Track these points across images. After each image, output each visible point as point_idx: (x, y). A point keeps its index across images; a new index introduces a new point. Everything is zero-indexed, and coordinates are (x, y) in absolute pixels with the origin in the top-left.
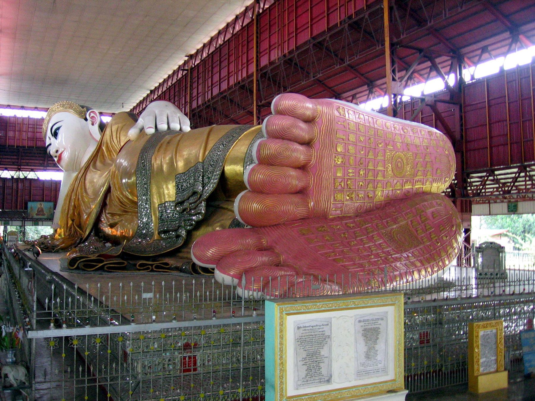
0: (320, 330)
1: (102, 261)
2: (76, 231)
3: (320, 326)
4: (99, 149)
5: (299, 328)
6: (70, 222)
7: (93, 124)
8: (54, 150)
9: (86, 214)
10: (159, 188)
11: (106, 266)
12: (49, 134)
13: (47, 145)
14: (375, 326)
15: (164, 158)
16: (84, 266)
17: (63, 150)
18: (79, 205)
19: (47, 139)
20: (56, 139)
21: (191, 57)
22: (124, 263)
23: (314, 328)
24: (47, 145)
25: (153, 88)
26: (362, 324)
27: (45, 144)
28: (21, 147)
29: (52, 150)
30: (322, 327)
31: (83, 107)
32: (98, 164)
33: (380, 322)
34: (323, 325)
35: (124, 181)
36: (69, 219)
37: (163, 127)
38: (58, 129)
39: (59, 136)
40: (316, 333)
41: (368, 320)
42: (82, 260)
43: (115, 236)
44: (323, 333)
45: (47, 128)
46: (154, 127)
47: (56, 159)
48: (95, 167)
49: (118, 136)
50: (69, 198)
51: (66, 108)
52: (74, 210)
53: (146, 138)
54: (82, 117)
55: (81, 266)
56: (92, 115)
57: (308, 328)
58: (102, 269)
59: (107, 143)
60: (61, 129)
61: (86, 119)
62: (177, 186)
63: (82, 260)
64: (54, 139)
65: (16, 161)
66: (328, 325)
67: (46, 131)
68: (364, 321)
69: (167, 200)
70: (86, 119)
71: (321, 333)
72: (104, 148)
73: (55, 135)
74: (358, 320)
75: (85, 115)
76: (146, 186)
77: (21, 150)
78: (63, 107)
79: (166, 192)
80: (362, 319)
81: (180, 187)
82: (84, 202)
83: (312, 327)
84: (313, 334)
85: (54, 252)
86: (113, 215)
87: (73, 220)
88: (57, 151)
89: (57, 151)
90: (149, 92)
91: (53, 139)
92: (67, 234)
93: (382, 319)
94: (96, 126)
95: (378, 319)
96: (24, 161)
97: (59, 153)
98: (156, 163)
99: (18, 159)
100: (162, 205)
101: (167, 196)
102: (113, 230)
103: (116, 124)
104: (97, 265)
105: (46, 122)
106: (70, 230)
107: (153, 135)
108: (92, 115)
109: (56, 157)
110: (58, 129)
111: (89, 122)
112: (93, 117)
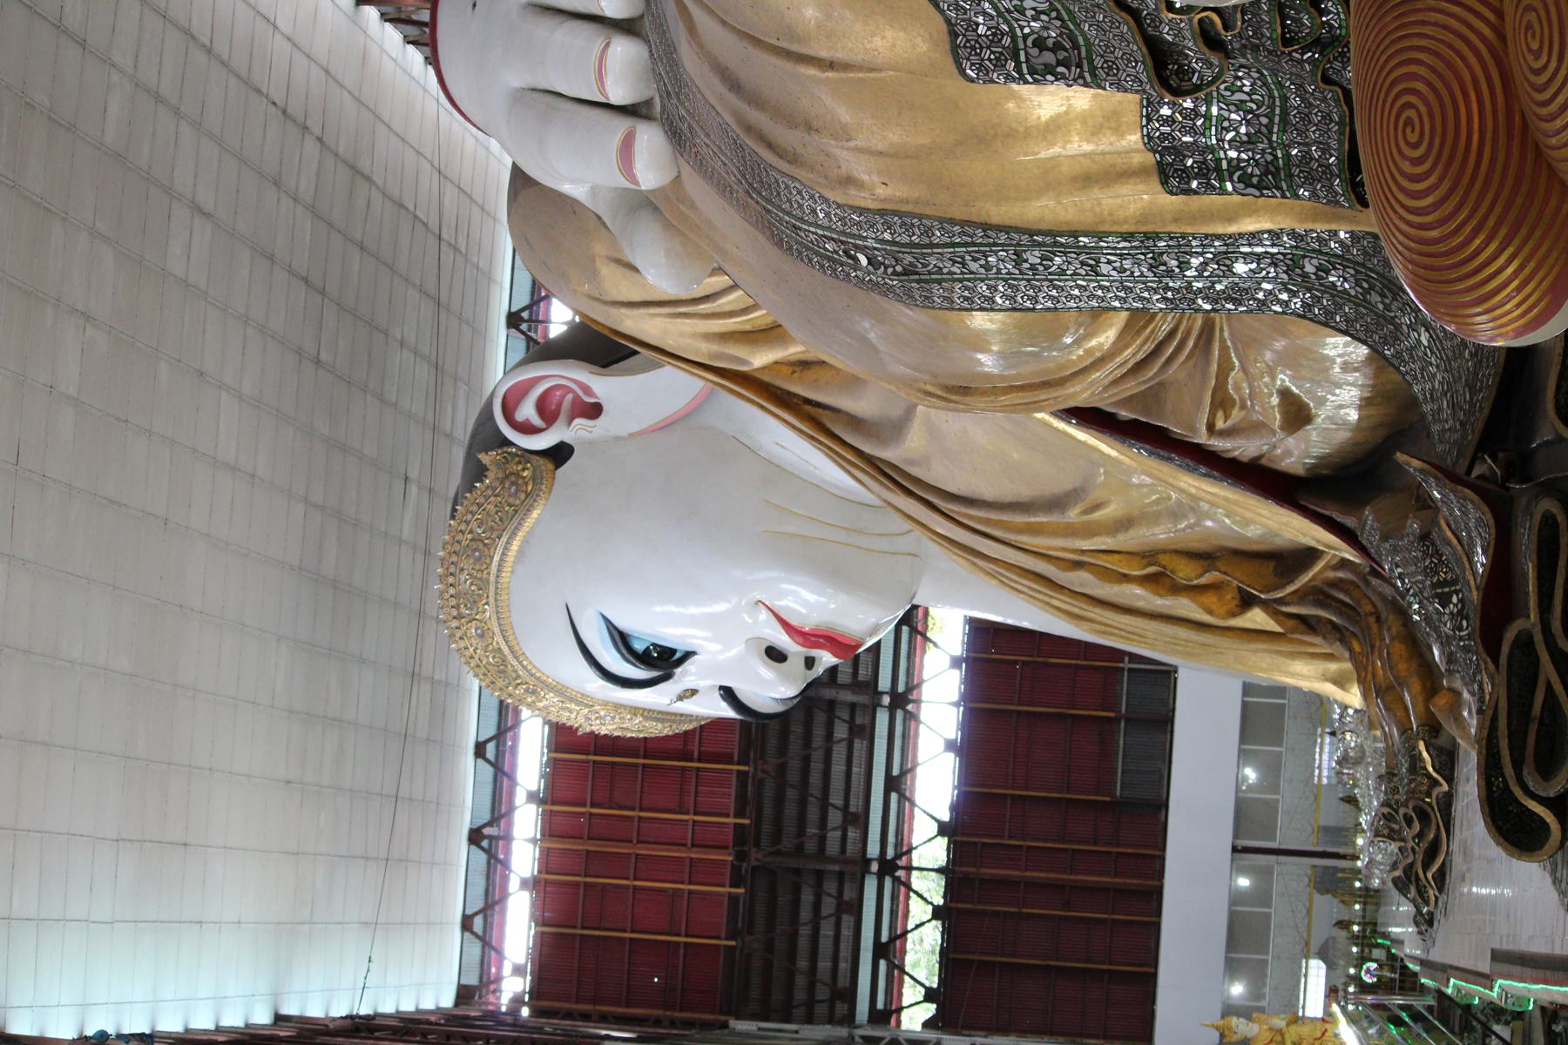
1: (1525, 644)
2: (1316, 594)
4: (768, 391)
6: (1257, 618)
7: (594, 411)
10: (1049, 179)
12: (658, 697)
13: (728, 712)
15: (843, 134)
17: (764, 615)
18: (1149, 555)
19: (687, 707)
20: (688, 655)
24: (728, 712)
27: (718, 724)
28: (741, 856)
29: (771, 690)
31: (475, 472)
32: (861, 405)
38: (621, 640)
39: (672, 635)
42: (1509, 770)
43: (1365, 404)
45: (618, 707)
46: (622, 124)
47: (827, 659)
51: (483, 584)
52: (1177, 589)
53: (699, 191)
56: (527, 411)
59: (725, 337)
62: (1040, 74)
63: (1509, 770)
64: (689, 666)
65: (831, 886)
67: (635, 710)
69: (1134, 139)
70: (560, 454)
72: (759, 359)
73: (663, 661)
76: (1033, 257)
77: (756, 856)
81: (1049, 58)
85: (1450, 780)
88: (775, 655)
89: (775, 655)
91: (686, 676)
92: (1337, 648)
96: (834, 836)
97: (783, 641)
98: (879, 188)
101: (1106, 143)
102: (1322, 415)
103: (594, 275)
104: (1549, 686)
106: (1308, 624)
108: (527, 411)
109: (810, 662)
110: (621, 640)
112: (542, 406)
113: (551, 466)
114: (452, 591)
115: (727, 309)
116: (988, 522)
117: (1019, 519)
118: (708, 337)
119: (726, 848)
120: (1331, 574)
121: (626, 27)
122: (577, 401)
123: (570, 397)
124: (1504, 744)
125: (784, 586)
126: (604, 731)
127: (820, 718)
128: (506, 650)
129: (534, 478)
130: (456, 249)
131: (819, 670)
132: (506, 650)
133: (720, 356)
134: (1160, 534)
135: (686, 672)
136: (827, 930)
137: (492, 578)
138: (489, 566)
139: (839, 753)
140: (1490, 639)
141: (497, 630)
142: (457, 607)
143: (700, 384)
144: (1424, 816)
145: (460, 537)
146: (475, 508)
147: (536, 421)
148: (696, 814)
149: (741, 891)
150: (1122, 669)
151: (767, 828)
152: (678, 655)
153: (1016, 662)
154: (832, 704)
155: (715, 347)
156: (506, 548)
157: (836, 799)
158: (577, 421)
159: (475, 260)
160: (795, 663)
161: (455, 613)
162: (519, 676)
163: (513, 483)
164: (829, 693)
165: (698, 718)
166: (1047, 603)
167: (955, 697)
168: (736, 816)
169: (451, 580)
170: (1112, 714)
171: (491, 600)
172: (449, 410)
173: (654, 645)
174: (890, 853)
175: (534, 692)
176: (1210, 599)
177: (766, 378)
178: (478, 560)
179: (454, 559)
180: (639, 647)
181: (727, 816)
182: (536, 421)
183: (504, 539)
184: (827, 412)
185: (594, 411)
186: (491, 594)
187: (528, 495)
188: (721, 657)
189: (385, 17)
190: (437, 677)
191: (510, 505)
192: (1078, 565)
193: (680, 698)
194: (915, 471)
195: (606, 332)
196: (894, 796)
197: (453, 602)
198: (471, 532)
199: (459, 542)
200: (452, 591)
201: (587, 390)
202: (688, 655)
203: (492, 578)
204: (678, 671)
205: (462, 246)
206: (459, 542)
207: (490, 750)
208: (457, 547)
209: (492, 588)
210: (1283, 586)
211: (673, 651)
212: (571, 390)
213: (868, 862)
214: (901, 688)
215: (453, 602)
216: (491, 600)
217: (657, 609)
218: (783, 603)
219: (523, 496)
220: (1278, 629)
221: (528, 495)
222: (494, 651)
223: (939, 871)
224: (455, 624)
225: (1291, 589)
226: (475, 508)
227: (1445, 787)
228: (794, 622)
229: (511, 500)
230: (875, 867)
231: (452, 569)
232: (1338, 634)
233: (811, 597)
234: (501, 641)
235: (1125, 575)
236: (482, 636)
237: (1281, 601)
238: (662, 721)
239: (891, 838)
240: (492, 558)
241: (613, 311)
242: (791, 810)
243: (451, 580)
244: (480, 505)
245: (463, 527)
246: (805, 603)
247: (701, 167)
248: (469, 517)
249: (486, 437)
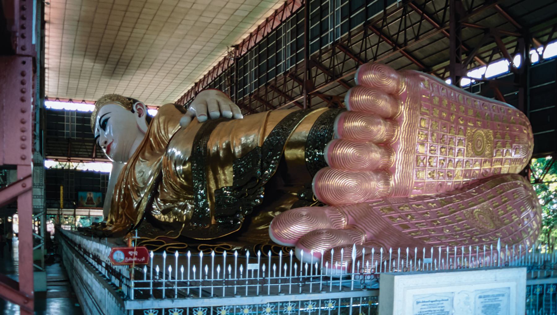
0: (440, 305)
3: (439, 301)
4: (147, 140)
5: (418, 303)
7: (140, 116)
8: (103, 141)
9: (137, 202)
14: (495, 303)
17: (111, 141)
21: (237, 47)
23: (434, 303)
25: (197, 81)
26: (482, 300)
29: (101, 141)
30: (441, 302)
31: (130, 99)
32: (147, 154)
33: (501, 298)
34: (443, 300)
35: (178, 168)
36: (120, 208)
37: (215, 114)
39: (108, 128)
40: (435, 309)
41: (488, 296)
44: (442, 309)
46: (206, 114)
47: (105, 151)
48: (144, 158)
49: (166, 127)
50: (402, 69)
51: (113, 100)
54: (129, 109)
56: (139, 107)
57: (428, 303)
64: (103, 131)
66: (447, 300)
67: (95, 122)
68: (485, 297)
71: (440, 309)
72: (151, 139)
73: (103, 126)
74: (478, 296)
75: (132, 106)
78: (110, 99)
79: (223, 177)
80: (482, 295)
83: (432, 302)
84: (432, 309)
88: (106, 142)
90: (193, 85)
91: (101, 131)
93: (503, 295)
94: (143, 118)
95: (499, 295)
97: (108, 144)
100: (219, 191)
102: (166, 217)
107: (205, 123)
108: (139, 107)
109: (105, 148)
110: (106, 120)
111: (136, 114)
121: (221, 115)
136: (60, 152)
139: (86, 153)
157: (80, 153)
185: (140, 116)
189: (192, 87)
247: (204, 125)
249: (135, 101)
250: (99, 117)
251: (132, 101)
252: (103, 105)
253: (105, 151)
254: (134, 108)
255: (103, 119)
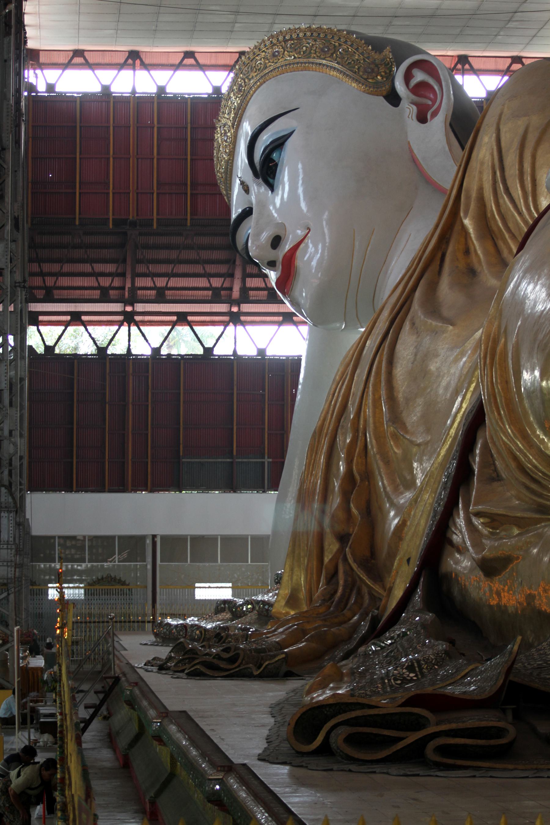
1: (417, 724)
2: (353, 584)
6: (332, 547)
7: (422, 119)
8: (265, 236)
9: (399, 510)
11: (432, 745)
16: (350, 740)
17: (300, 233)
18: (368, 476)
20: (272, 187)
22: (499, 732)
24: (234, 216)
27: (228, 209)
28: (133, 224)
31: (378, 44)
38: (279, 144)
39: (285, 177)
43: (502, 609)
47: (273, 276)
48: (433, 308)
51: (307, 54)
52: (346, 495)
54: (373, 89)
55: (338, 739)
56: (419, 76)
58: (414, 756)
59: (481, 199)
60: (289, 144)
61: (393, 98)
64: (264, 188)
65: (117, 282)
67: (232, 154)
70: (393, 98)
73: (266, 170)
75: (391, 78)
78: (295, 48)
82: (387, 462)
86: (495, 521)
87: (343, 538)
88: (276, 242)
89: (276, 242)
94: (438, 124)
96: (147, 282)
99: (123, 275)
102: (496, 585)
104: (401, 739)
105: (226, 118)
106: (332, 577)
108: (419, 76)
109: (272, 264)
110: (279, 144)
111: (408, 109)
112: (422, 85)
113: (385, 93)
114: (301, 35)
115: (501, 201)
116: (378, 373)
117: (383, 393)
118: (481, 190)
119: (137, 215)
120: (365, 590)
122: (429, 107)
123: (430, 103)
124: (358, 713)
125: (320, 246)
126: (217, 136)
127: (223, 269)
128: (266, 71)
129: (377, 82)
130: (509, 21)
131: (267, 271)
132: (266, 71)
133: (468, 198)
134: (382, 483)
135: (259, 185)
137: (311, 60)
138: (319, 57)
140: (412, 701)
141: (278, 65)
142: (292, 39)
143: (447, 186)
144: (233, 660)
145: (336, 38)
146: (355, 46)
147: (413, 82)
148: (158, 194)
149: (111, 226)
150: (264, 458)
151: (152, 240)
152: (271, 180)
153: (264, 390)
154: (232, 276)
155: (474, 194)
156: (331, 67)
158: (415, 108)
159: (502, 33)
160: (272, 254)
161: (287, 37)
162: (250, 80)
163: (373, 70)
164: (238, 274)
165: (229, 196)
166: (327, 413)
167: (240, 352)
168: (158, 219)
169: (308, 34)
170: (235, 453)
171: (298, 60)
172: (408, 23)
173: (276, 165)
174: (137, 318)
175: (240, 90)
176: (341, 515)
177: (457, 228)
178: (322, 50)
179: (322, 35)
180: (275, 155)
181: (158, 214)
182: (413, 82)
183: (336, 66)
184: (438, 267)
185: (422, 119)
186: (301, 60)
187: (366, 79)
188: (271, 208)
190: (237, 25)
191: (358, 69)
192: (356, 430)
193: (242, 183)
194: (407, 326)
195: (477, 125)
196: (174, 318)
197: (294, 36)
198: (340, 45)
199: (333, 37)
200: (301, 35)
201: (435, 114)
202: (272, 187)
203: (311, 60)
204: (260, 180)
205: (511, 25)
206: (333, 37)
207: (191, 61)
208: (329, 37)
209: (305, 60)
210: (355, 561)
211: (274, 178)
212: (434, 102)
213: (132, 305)
214: (243, 318)
215: (294, 36)
216: (298, 60)
217: (300, 166)
218: (311, 246)
219: (365, 77)
220: (326, 560)
221: (366, 79)
222: (265, 64)
223: (129, 350)
224: (281, 38)
225: (354, 566)
226: (355, 46)
227: (256, 673)
228: (299, 253)
229: (362, 69)
230: (129, 309)
231: (315, 34)
232: (329, 597)
233: (314, 263)
234: (272, 68)
235: (352, 461)
236: (274, 55)
237: (345, 559)
238: (226, 172)
239: (147, 318)
240: (324, 59)
241: (493, 129)
242: (163, 254)
243: (308, 34)
244: (357, 49)
245: (342, 40)
246: (311, 259)
248: (349, 43)
249: (401, 51)
250: (247, 128)
251: (387, 53)
252: (263, 80)
253: (273, 276)
254: (400, 86)
255: (265, 139)
